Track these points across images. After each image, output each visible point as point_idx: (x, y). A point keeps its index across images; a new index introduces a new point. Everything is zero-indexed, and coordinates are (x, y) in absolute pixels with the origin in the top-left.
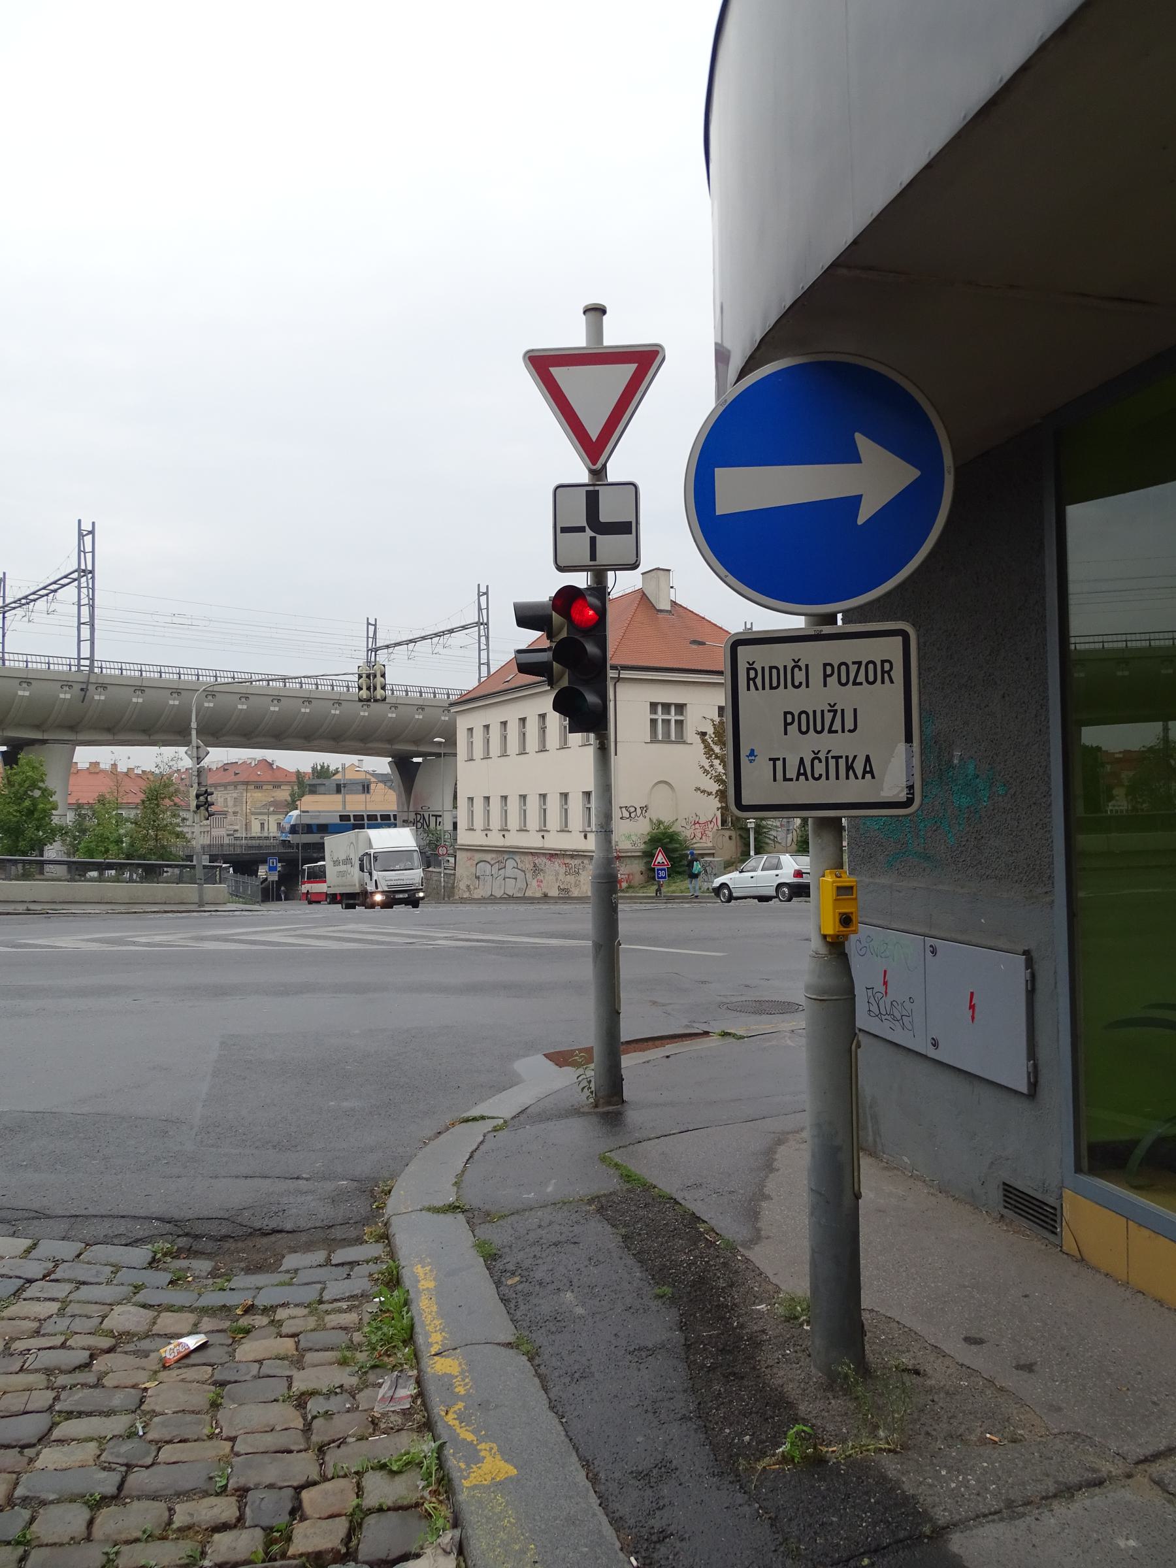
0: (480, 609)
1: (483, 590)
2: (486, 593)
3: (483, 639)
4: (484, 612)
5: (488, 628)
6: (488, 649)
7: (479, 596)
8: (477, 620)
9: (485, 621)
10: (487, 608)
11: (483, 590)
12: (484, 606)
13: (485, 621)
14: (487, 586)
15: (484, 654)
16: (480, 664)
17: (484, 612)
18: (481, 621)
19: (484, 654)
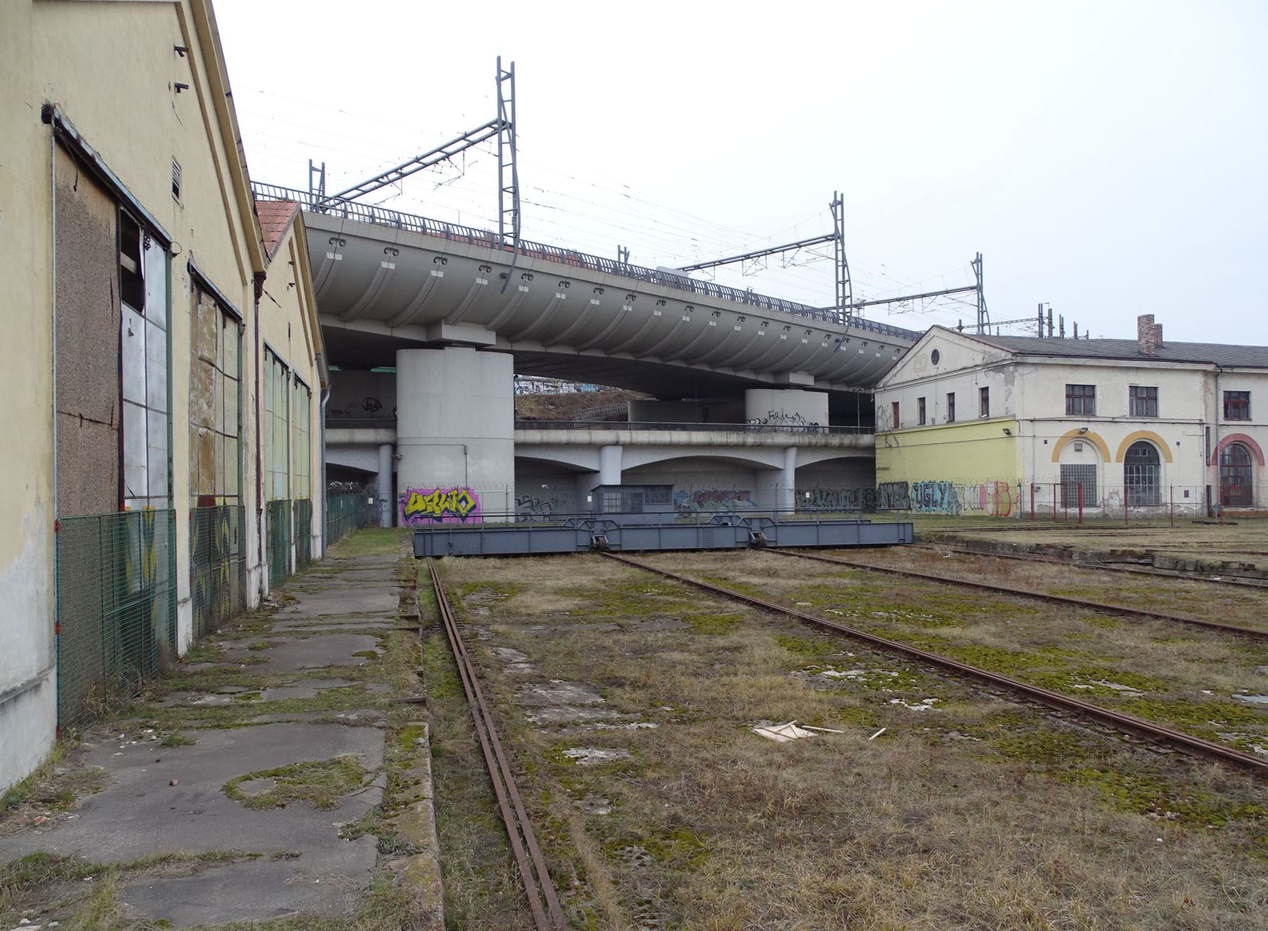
0: (501, 102)
1: (506, 67)
2: (511, 76)
3: (507, 149)
4: (508, 106)
6: (514, 164)
8: (495, 117)
9: (510, 120)
10: (513, 101)
11: (506, 67)
12: (507, 95)
13: (510, 120)
14: (513, 64)
15: (507, 172)
16: (502, 190)
18: (503, 119)
19: (507, 172)
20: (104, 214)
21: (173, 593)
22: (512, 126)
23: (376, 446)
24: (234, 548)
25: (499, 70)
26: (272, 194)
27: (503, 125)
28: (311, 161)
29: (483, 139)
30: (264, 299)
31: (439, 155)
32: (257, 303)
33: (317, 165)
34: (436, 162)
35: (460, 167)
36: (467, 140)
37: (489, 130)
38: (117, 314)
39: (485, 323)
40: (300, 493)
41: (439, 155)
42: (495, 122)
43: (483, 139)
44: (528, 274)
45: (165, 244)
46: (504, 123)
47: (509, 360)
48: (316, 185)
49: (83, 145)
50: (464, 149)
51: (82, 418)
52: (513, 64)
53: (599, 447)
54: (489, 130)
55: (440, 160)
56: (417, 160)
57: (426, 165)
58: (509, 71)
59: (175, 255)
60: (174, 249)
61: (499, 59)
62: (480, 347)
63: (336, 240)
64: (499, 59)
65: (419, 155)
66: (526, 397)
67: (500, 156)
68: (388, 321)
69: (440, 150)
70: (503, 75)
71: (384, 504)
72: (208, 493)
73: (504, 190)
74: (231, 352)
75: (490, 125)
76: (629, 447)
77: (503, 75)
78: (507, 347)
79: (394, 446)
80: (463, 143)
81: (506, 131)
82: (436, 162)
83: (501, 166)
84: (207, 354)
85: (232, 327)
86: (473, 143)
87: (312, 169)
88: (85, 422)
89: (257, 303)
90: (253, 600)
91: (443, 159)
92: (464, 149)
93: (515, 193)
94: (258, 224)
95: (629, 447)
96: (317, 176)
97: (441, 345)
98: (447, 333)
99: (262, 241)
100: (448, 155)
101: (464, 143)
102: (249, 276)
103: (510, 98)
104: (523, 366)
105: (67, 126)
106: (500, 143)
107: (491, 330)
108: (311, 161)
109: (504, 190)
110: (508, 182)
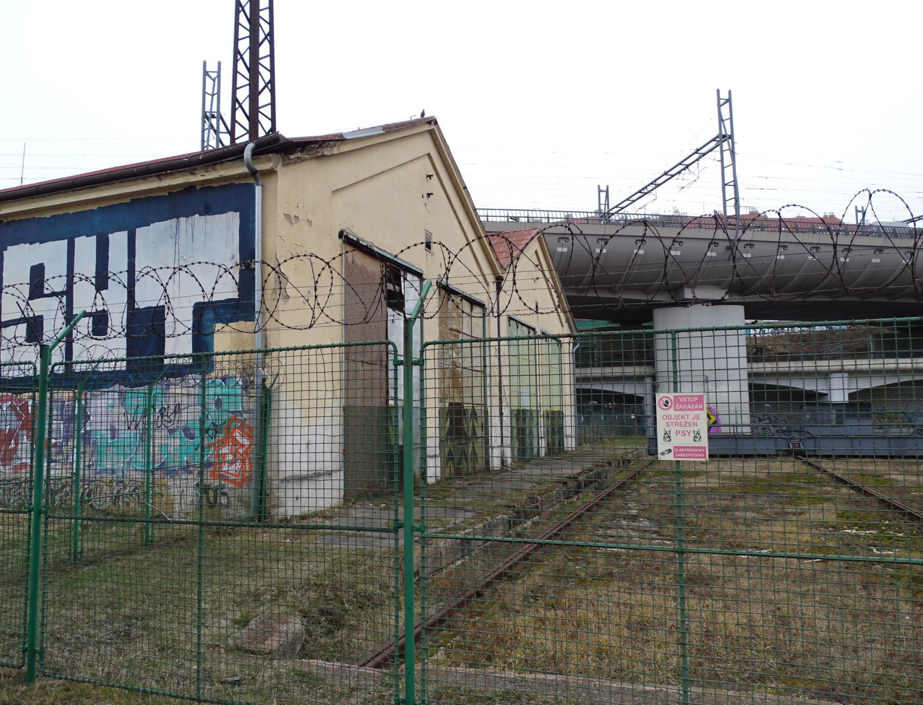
0: (721, 120)
1: (724, 95)
2: (729, 101)
4: (727, 123)
5: (733, 143)
6: (734, 164)
7: (719, 106)
8: (717, 133)
10: (731, 118)
11: (724, 95)
13: (729, 133)
14: (730, 92)
15: (729, 172)
16: (724, 185)
17: (727, 123)
18: (723, 133)
19: (729, 172)
20: (375, 268)
21: (424, 448)
22: (731, 137)
23: (640, 378)
24: (479, 433)
25: (719, 99)
26: (559, 216)
27: (722, 138)
28: (599, 186)
29: (711, 150)
30: (502, 293)
31: (681, 167)
32: (498, 294)
33: (603, 188)
34: (679, 172)
35: (696, 173)
36: (699, 153)
37: (713, 144)
38: (384, 313)
39: (718, 285)
40: (546, 404)
41: (681, 167)
42: (717, 137)
43: (711, 150)
44: (750, 244)
45: (419, 275)
46: (724, 136)
47: (740, 309)
48: (603, 201)
49: (361, 242)
50: (698, 160)
51: (363, 362)
52: (730, 92)
53: (826, 375)
54: (713, 144)
55: (682, 170)
56: (666, 174)
57: (673, 176)
58: (727, 97)
59: (424, 279)
60: (424, 277)
61: (718, 91)
62: (715, 303)
63: (602, 239)
64: (718, 91)
65: (667, 170)
66: (781, 336)
67: (722, 161)
68: (644, 290)
69: (680, 164)
70: (722, 102)
71: (648, 419)
72: (457, 401)
73: (726, 185)
74: (477, 324)
75: (714, 140)
76: (854, 374)
77: (722, 102)
78: (737, 298)
79: (654, 377)
80: (696, 156)
81: (726, 142)
82: (679, 172)
83: (723, 168)
84: (454, 327)
85: (477, 311)
86: (704, 154)
87: (600, 191)
88: (365, 364)
89: (498, 294)
90: (496, 463)
91: (684, 169)
92: (698, 160)
93: (735, 186)
94: (493, 251)
95: (854, 374)
96: (603, 195)
97: (686, 303)
98: (688, 294)
99: (498, 259)
100: (687, 166)
101: (696, 156)
102: (491, 278)
103: (729, 117)
104: (752, 312)
105: (351, 237)
106: (722, 152)
107: (723, 288)
108: (599, 186)
109: (726, 185)
110: (729, 178)
